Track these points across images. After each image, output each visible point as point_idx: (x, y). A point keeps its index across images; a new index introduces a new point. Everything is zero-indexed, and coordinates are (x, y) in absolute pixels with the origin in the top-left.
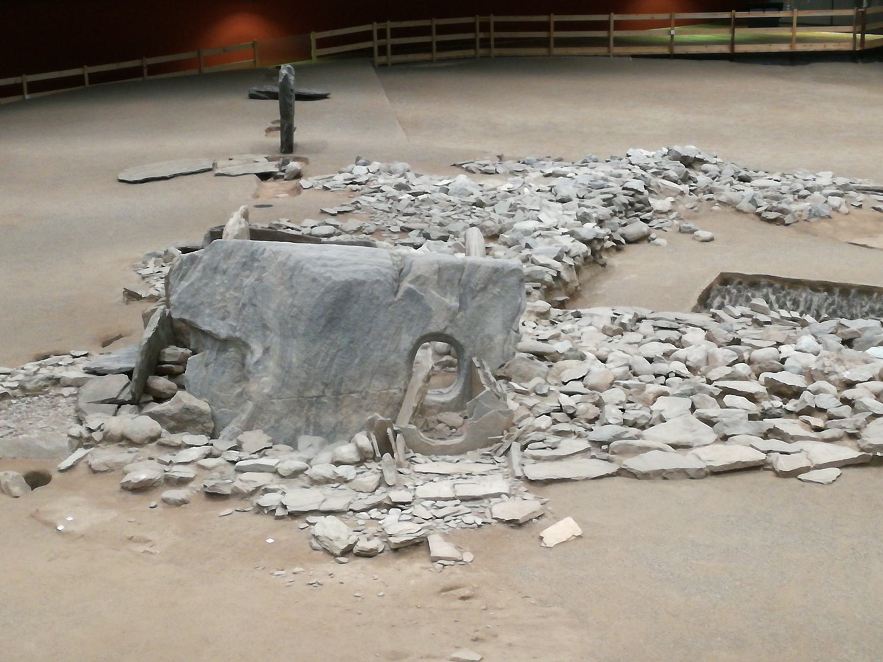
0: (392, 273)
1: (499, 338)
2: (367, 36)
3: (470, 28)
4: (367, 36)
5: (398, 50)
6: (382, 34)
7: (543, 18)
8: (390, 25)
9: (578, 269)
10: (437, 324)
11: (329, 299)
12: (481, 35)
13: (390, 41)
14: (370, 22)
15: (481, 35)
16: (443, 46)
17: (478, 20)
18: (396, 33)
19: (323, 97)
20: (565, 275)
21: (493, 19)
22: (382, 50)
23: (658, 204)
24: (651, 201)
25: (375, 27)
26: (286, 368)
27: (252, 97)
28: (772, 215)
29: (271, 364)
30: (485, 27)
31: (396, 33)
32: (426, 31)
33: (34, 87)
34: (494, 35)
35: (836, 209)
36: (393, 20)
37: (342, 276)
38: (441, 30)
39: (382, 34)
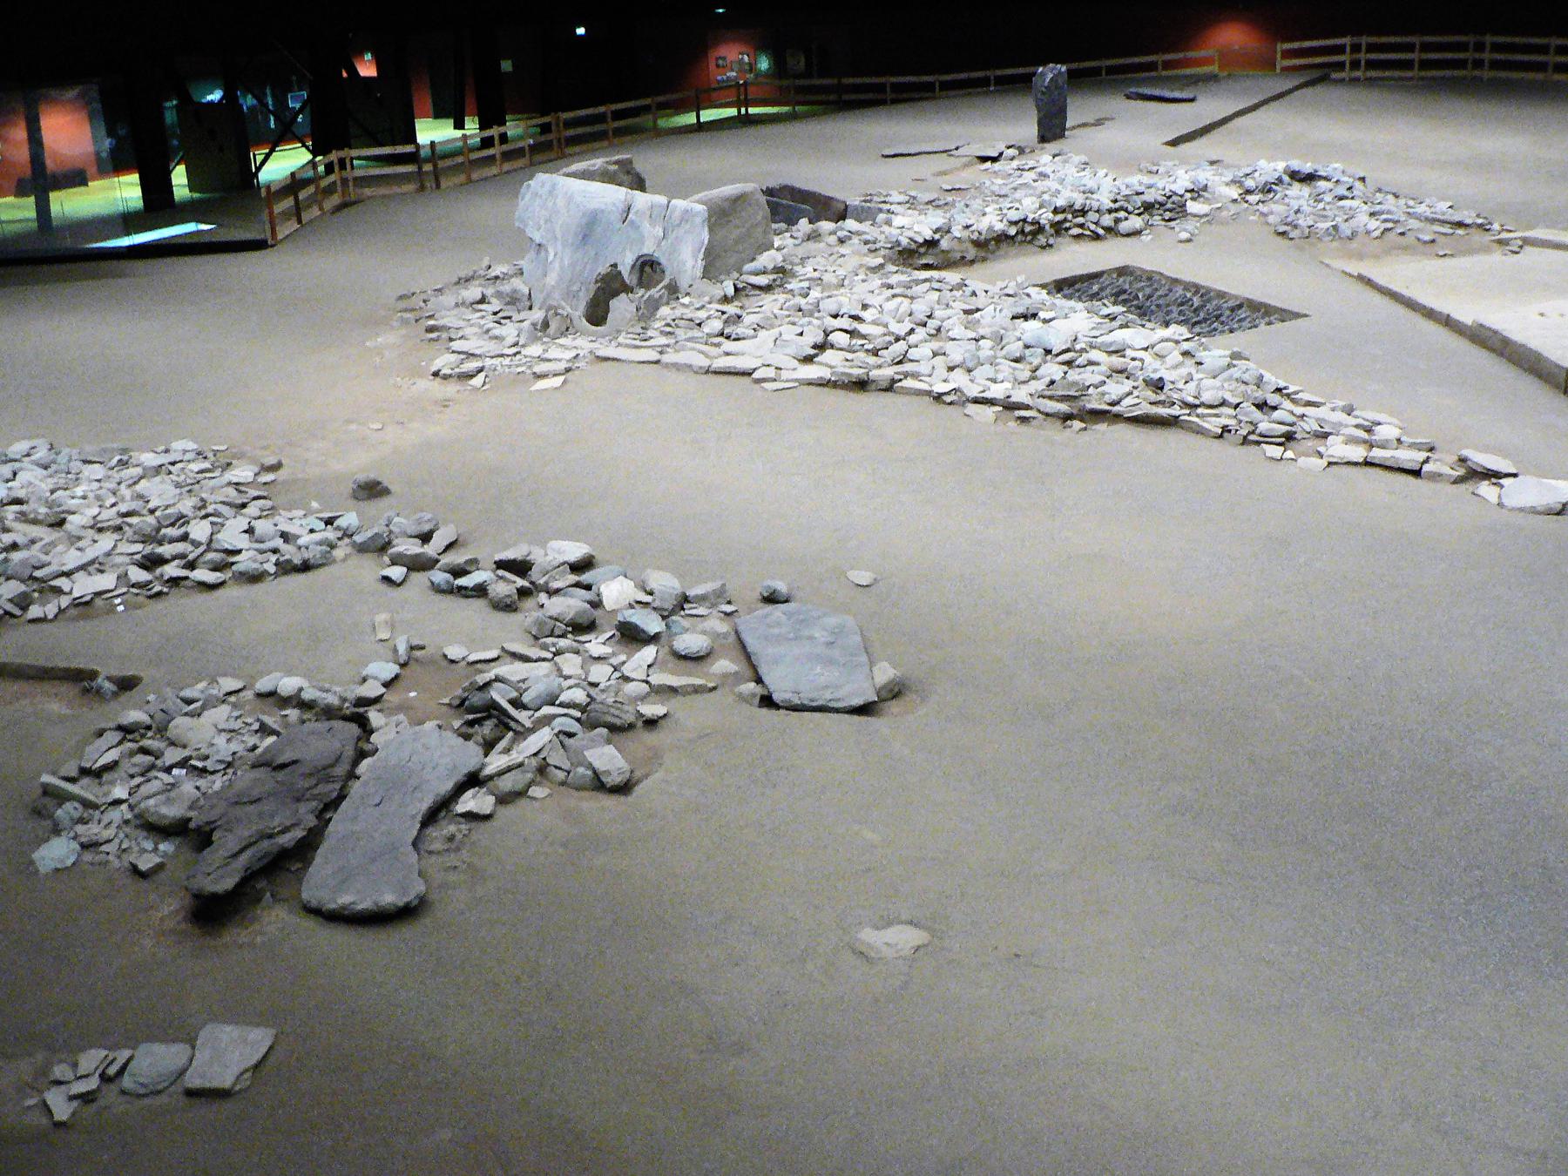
0: (621, 206)
1: (690, 263)
2: (1340, 50)
3: (1462, 47)
4: (1340, 50)
5: (1371, 65)
6: (1356, 48)
8: (1364, 40)
9: (978, 244)
10: (648, 248)
11: (584, 221)
13: (1363, 56)
14: (1344, 35)
16: (1425, 65)
19: (1192, 100)
20: (944, 244)
21: (1489, 39)
22: (1355, 65)
23: (1193, 207)
24: (1189, 203)
26: (562, 268)
27: (1128, 97)
28: (1281, 229)
29: (557, 265)
31: (1372, 48)
32: (1409, 48)
33: (1001, 81)
35: (1368, 233)
36: (1370, 34)
37: (594, 205)
38: (1426, 47)
39: (1356, 48)
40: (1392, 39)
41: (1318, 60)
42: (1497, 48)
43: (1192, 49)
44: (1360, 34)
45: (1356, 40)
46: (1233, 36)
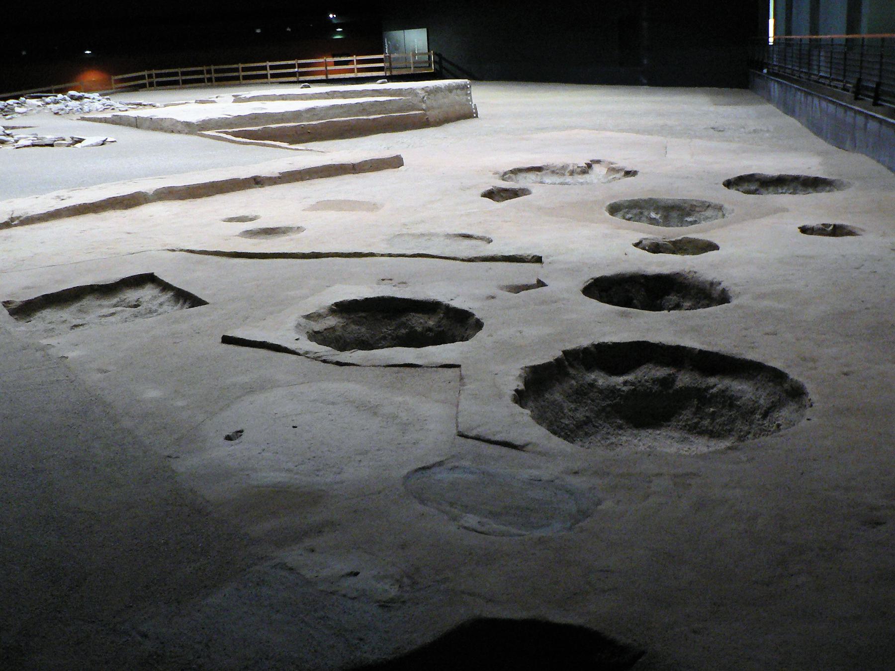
2: (143, 77)
3: (201, 72)
4: (143, 77)
6: (150, 76)
7: (235, 66)
8: (154, 72)
12: (208, 76)
13: (155, 80)
15: (208, 76)
17: (205, 68)
18: (158, 76)
25: (145, 73)
30: (209, 72)
31: (158, 76)
32: (176, 74)
34: (214, 75)
38: (183, 74)
40: (167, 71)
41: (132, 83)
42: (216, 71)
43: (69, 82)
44: (151, 69)
45: (149, 72)
46: (92, 76)
